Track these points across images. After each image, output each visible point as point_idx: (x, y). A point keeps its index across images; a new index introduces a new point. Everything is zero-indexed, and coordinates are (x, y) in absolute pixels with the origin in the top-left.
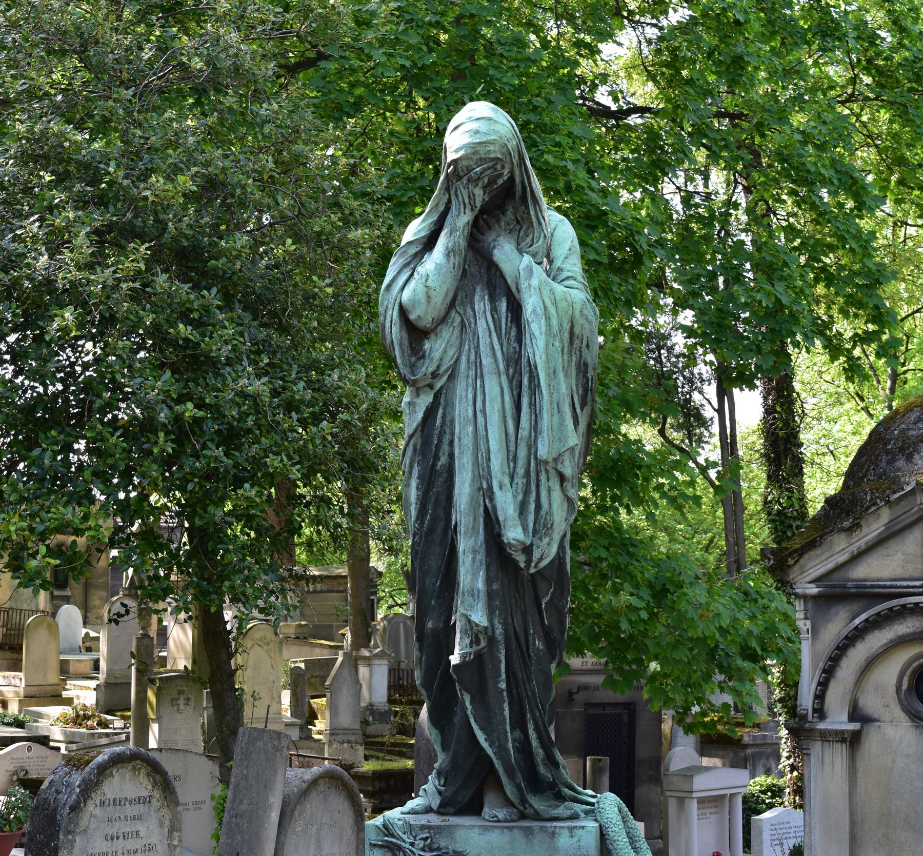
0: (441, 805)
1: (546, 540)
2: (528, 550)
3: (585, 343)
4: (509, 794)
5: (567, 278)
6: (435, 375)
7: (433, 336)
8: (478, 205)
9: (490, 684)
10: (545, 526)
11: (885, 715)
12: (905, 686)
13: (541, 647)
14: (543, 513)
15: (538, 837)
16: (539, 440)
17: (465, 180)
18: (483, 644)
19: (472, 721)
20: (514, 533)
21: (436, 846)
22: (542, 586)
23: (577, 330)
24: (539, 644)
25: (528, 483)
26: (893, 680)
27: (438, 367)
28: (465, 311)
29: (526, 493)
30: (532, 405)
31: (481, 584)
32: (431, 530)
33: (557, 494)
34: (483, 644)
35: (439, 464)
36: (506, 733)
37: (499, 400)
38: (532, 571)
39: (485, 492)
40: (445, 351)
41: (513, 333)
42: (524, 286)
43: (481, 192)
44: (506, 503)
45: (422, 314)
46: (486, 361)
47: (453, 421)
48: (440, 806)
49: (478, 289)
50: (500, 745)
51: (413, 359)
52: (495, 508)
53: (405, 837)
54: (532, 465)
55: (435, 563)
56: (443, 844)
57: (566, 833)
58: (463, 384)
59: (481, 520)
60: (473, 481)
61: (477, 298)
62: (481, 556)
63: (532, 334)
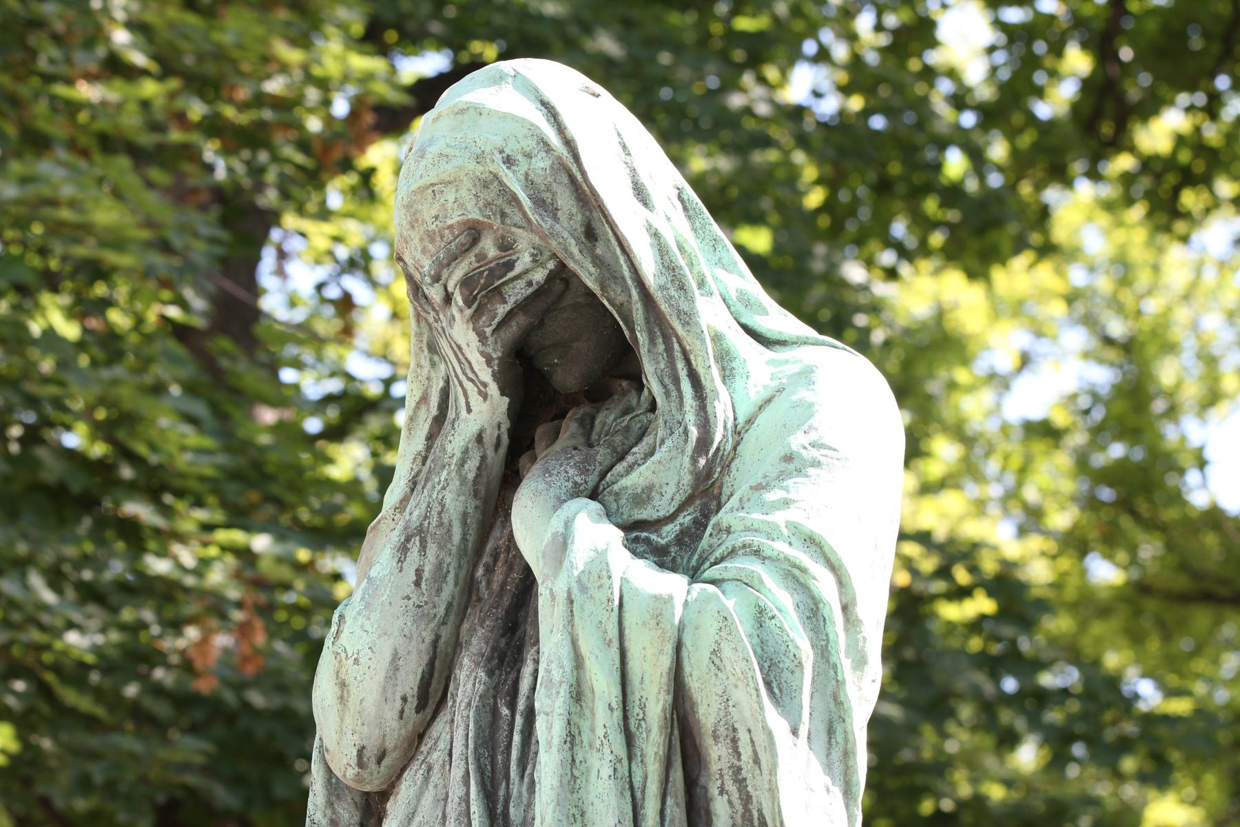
5: (732, 553)
8: (486, 375)
23: (707, 714)
43: (473, 337)
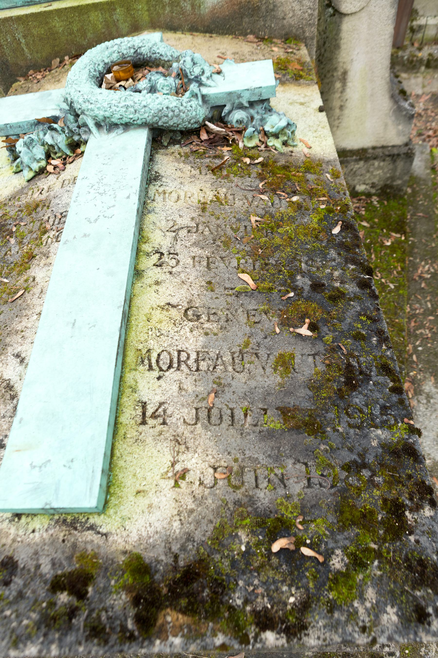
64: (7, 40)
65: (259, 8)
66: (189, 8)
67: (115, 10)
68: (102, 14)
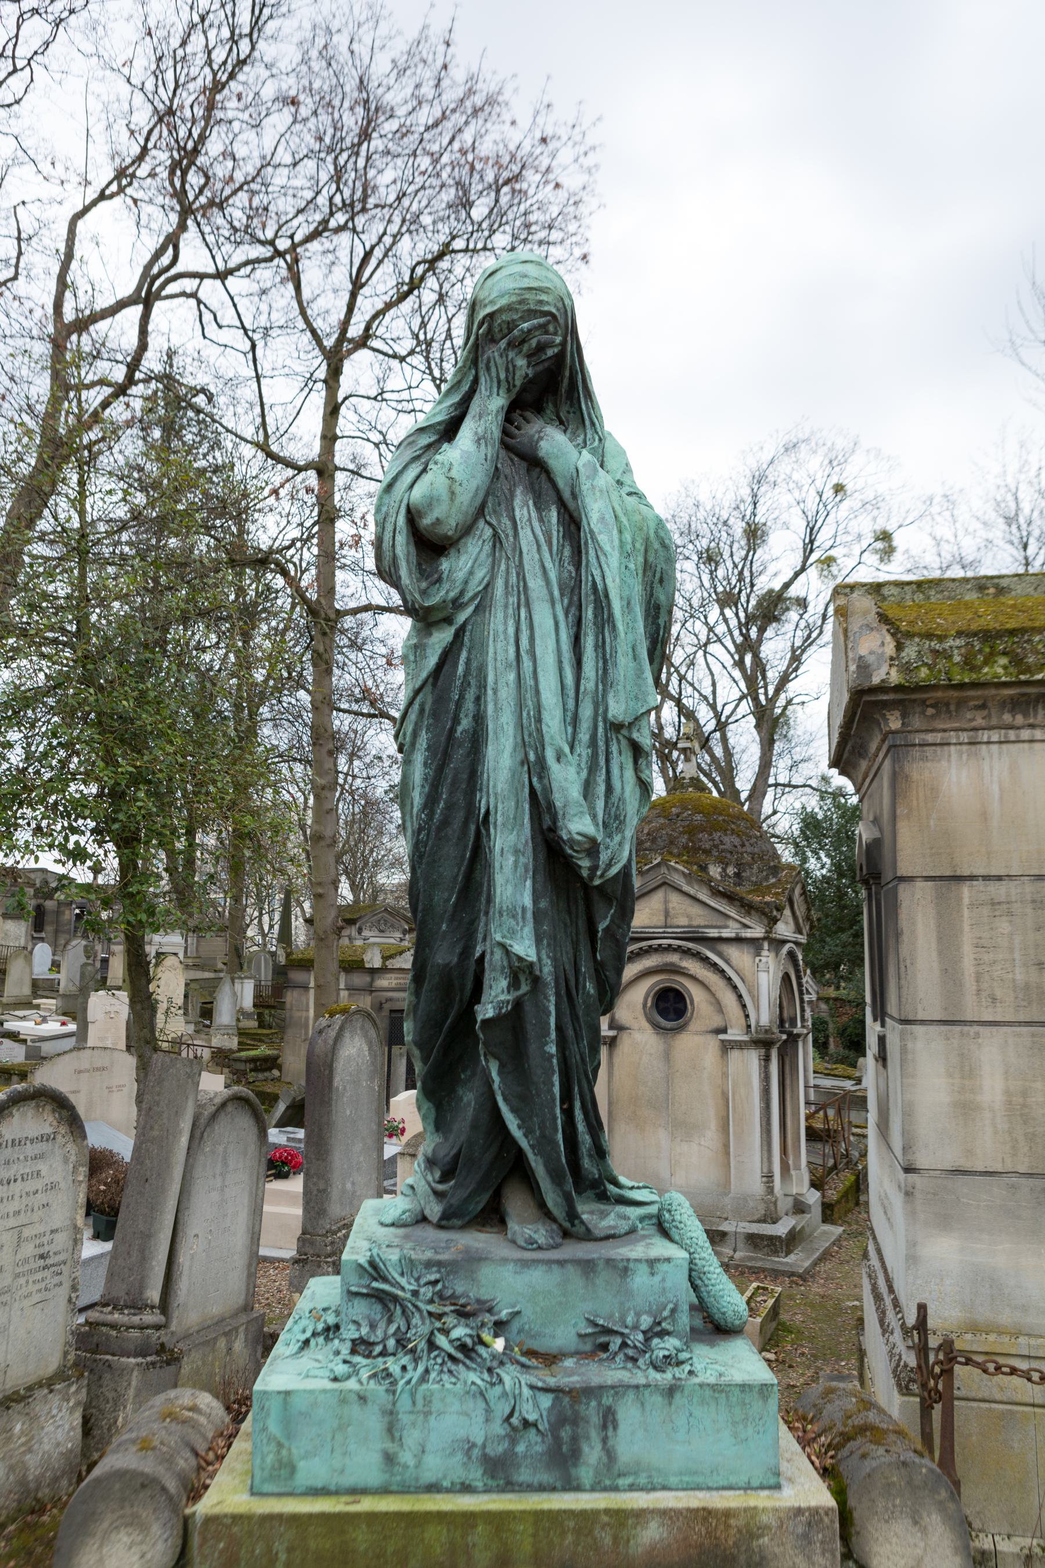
0: (446, 1216)
1: (617, 838)
2: (593, 848)
3: (658, 575)
4: (550, 1204)
6: (457, 604)
7: (453, 552)
8: (518, 383)
9: (533, 1047)
10: (617, 817)
11: (635, 1026)
12: (649, 1004)
13: (592, 991)
14: (614, 799)
15: (603, 1277)
16: (611, 695)
17: (503, 344)
18: (525, 988)
19: (500, 1099)
20: (578, 825)
21: (450, 1292)
22: (599, 906)
24: (590, 987)
25: (594, 756)
26: (641, 1000)
27: (462, 593)
28: (499, 522)
29: (592, 769)
30: (600, 646)
31: (527, 900)
32: (445, 822)
33: (629, 774)
34: (525, 988)
35: (460, 729)
36: (555, 1118)
37: (553, 636)
38: (597, 882)
39: (534, 767)
40: (471, 573)
41: (567, 552)
42: (585, 486)
44: (566, 779)
45: (445, 516)
46: (535, 584)
47: (482, 669)
48: (441, 1219)
49: (519, 492)
50: (543, 1136)
51: (424, 585)
52: (548, 790)
53: (403, 1281)
54: (600, 730)
55: (451, 869)
56: (460, 1289)
57: (644, 1268)
58: (500, 615)
59: (527, 806)
60: (515, 750)
61: (517, 502)
62: (527, 858)
63: (598, 548)
64: (253, 1551)
65: (734, 1558)
66: (608, 1540)
67: (474, 1526)
68: (448, 1530)
